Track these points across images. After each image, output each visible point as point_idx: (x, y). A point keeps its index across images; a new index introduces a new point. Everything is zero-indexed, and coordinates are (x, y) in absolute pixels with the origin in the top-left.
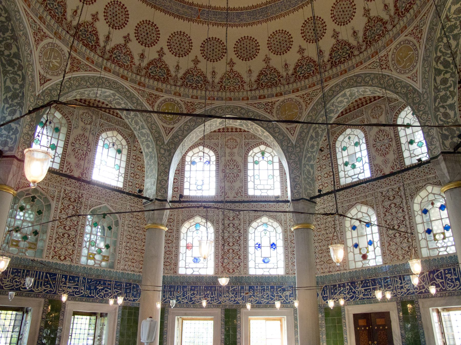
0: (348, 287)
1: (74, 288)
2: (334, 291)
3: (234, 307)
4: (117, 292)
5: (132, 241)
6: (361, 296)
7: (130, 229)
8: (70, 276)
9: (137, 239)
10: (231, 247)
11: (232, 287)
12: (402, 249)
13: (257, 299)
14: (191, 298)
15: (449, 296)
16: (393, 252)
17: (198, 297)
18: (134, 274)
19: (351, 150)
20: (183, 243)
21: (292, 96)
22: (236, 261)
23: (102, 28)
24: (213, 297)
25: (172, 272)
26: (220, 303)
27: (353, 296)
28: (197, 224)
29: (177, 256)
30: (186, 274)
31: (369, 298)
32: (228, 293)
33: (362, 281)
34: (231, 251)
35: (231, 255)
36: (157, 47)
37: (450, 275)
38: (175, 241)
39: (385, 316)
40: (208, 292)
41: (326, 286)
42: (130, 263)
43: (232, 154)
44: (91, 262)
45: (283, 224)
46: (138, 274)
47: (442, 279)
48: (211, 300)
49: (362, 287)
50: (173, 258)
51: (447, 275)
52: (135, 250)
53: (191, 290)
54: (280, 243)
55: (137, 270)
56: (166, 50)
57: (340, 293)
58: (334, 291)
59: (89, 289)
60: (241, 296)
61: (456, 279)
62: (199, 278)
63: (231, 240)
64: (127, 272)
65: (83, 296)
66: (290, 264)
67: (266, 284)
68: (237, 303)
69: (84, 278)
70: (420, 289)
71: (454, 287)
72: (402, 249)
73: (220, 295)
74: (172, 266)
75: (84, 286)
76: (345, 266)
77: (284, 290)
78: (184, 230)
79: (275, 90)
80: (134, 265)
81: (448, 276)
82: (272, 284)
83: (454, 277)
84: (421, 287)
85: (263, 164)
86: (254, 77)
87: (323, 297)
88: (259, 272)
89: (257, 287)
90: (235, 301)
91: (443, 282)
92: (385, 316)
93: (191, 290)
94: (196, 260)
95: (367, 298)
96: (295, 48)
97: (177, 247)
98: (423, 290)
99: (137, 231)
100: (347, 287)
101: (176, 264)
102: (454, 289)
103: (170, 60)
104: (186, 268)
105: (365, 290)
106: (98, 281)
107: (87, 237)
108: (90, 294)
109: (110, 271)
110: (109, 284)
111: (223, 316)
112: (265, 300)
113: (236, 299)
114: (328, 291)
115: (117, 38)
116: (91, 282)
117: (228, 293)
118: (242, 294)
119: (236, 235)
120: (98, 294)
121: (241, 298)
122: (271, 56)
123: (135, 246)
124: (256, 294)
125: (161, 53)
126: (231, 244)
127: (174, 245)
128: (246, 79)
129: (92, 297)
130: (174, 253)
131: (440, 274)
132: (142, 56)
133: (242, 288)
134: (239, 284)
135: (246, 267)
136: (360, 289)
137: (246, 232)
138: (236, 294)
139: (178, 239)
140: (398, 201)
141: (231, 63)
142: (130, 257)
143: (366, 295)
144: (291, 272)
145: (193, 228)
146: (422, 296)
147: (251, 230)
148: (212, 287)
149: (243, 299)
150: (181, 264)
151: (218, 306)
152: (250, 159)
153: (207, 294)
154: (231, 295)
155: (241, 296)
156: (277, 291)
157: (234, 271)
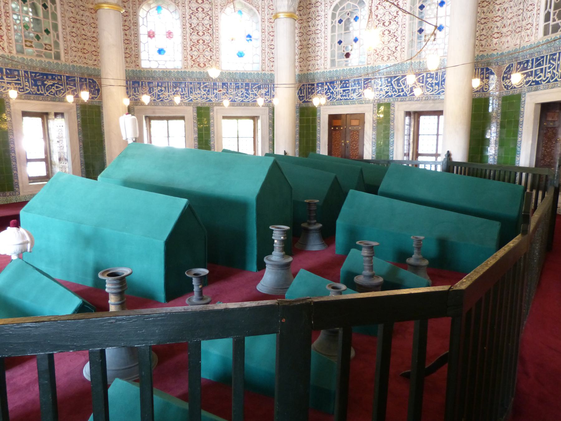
0: (327, 87)
1: (16, 84)
2: (312, 90)
3: (207, 105)
4: (71, 88)
5: (78, 25)
6: (339, 97)
7: (73, 10)
8: (6, 69)
9: (84, 23)
11: (204, 83)
12: (389, 48)
13: (231, 96)
14: (159, 95)
15: (425, 100)
16: (378, 52)
17: (167, 93)
18: (87, 68)
20: (143, 31)
22: (207, 53)
24: (184, 94)
25: (133, 65)
26: (191, 100)
27: (331, 97)
29: (137, 45)
30: (150, 68)
31: (347, 99)
32: (200, 89)
33: (341, 82)
34: (201, 42)
35: (201, 47)
37: (431, 79)
38: (132, 27)
39: (361, 117)
40: (178, 89)
41: (303, 85)
42: (80, 54)
45: (260, 12)
46: (93, 67)
47: (423, 83)
49: (341, 88)
50: (134, 48)
51: (428, 80)
52: (84, 37)
53: (158, 85)
54: (256, 35)
55: (91, 62)
57: (318, 93)
58: (312, 90)
59: (36, 85)
60: (214, 93)
61: (436, 84)
62: (166, 73)
63: (201, 28)
64: (78, 65)
65: (29, 93)
66: (267, 59)
67: (240, 80)
68: (210, 101)
69: (26, 72)
70: (399, 92)
71: (432, 91)
72: (389, 48)
74: (133, 59)
75: (29, 83)
76: (326, 64)
77: (259, 88)
78: (142, 12)
80: (86, 56)
81: (429, 80)
82: (247, 81)
83: (435, 81)
84: (400, 90)
87: (300, 97)
89: (231, 84)
90: (207, 98)
91: (423, 86)
92: (361, 117)
93: (158, 85)
94: (160, 51)
95: (345, 99)
97: (137, 35)
98: (402, 94)
99: (82, 12)
100: (325, 87)
101: (137, 56)
102: (432, 93)
104: (150, 61)
105: (344, 91)
106: (45, 75)
108: (38, 91)
109: (57, 64)
110: (59, 79)
111: (195, 114)
112: (240, 98)
113: (209, 97)
114: (305, 90)
116: (35, 76)
117: (200, 89)
118: (215, 91)
119: (206, 22)
120: (47, 91)
121: (213, 96)
123: (83, 32)
124: (229, 91)
126: (201, 34)
127: (133, 33)
129: (41, 94)
130: (133, 43)
131: (421, 78)
136: (339, 89)
138: (209, 91)
139: (136, 24)
142: (80, 46)
143: (344, 96)
144: (267, 69)
145: (154, 11)
146: (399, 100)
149: (216, 97)
150: (143, 55)
151: (189, 104)
153: (176, 91)
155: (214, 93)
156: (251, 89)
157: (205, 65)
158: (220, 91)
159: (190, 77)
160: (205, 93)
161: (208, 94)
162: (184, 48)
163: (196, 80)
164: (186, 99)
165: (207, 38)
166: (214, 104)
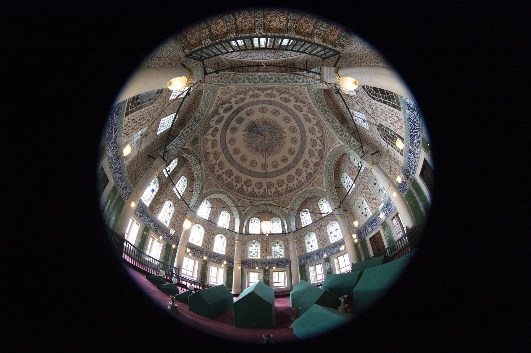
10: (322, 237)
19: (346, 181)
21: (318, 176)
23: (256, 190)
28: (309, 235)
29: (305, 247)
36: (274, 187)
43: (313, 207)
44: (276, 257)
56: (277, 187)
79: (312, 178)
85: (324, 204)
86: (305, 179)
88: (334, 241)
96: (310, 162)
97: (305, 244)
101: (306, 250)
103: (280, 189)
107: (273, 250)
115: (262, 191)
122: (306, 169)
125: (276, 188)
128: (303, 181)
132: (271, 192)
135: (329, 241)
137: (326, 230)
139: (304, 242)
140: (366, 187)
141: (297, 179)
147: (327, 228)
152: (319, 205)
162: (318, 243)
165: (324, 237)
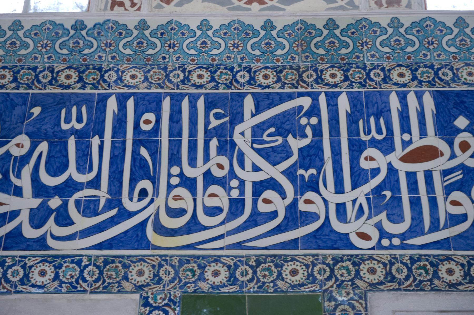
3: (293, 275)
11: (262, 103)
24: (70, 187)
26: (137, 237)
32: (227, 147)
48: (38, 218)
73: (141, 170)
113: (312, 203)
117: (227, 147)
118: (374, 159)
133: (368, 107)
134: (333, 76)
148: (62, 101)
149: (385, 200)
154: (255, 168)
158: (429, 153)
159: (146, 64)
160: (271, 171)
161: (313, 185)
163: (200, 77)
164: (82, 223)
166: (372, 273)
